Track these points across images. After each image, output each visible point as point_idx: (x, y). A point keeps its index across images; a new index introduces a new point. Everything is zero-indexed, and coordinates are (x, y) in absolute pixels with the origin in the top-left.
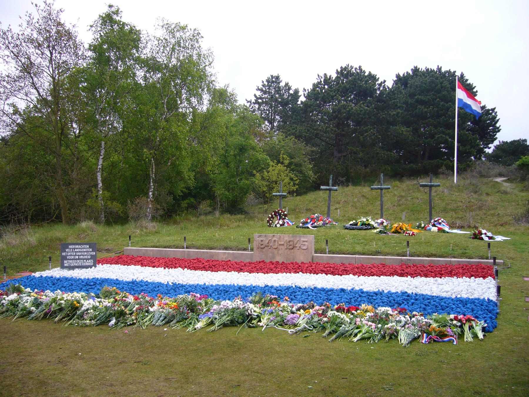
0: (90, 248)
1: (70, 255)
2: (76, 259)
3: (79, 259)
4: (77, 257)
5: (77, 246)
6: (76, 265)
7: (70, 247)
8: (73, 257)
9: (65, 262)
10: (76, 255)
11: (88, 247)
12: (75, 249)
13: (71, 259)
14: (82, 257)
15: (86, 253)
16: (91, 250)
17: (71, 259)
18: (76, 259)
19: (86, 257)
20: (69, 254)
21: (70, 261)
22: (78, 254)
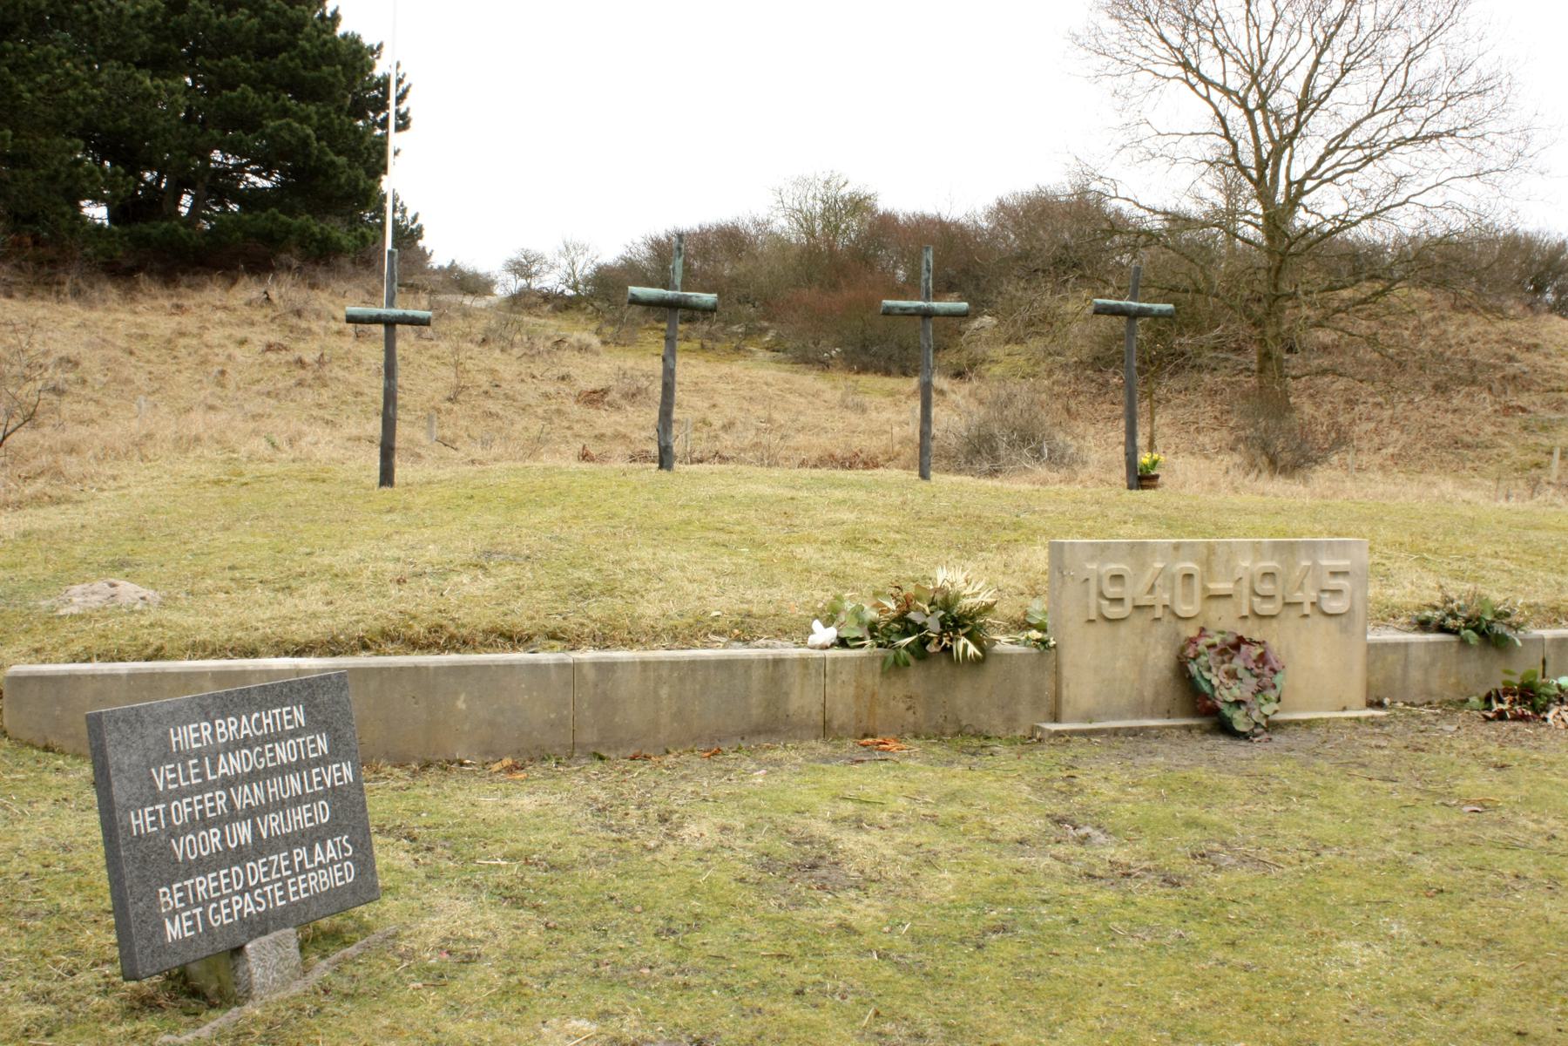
0: (314, 725)
1: (200, 823)
2: (240, 855)
3: (260, 847)
4: (244, 832)
5: (228, 728)
6: (247, 905)
7: (186, 736)
8: (213, 838)
9: (169, 897)
10: (233, 815)
11: (299, 716)
12: (213, 753)
13: (203, 866)
14: (273, 824)
15: (294, 783)
16: (323, 745)
17: (203, 866)
18: (240, 855)
19: (300, 817)
20: (182, 810)
21: (203, 884)
22: (246, 796)
